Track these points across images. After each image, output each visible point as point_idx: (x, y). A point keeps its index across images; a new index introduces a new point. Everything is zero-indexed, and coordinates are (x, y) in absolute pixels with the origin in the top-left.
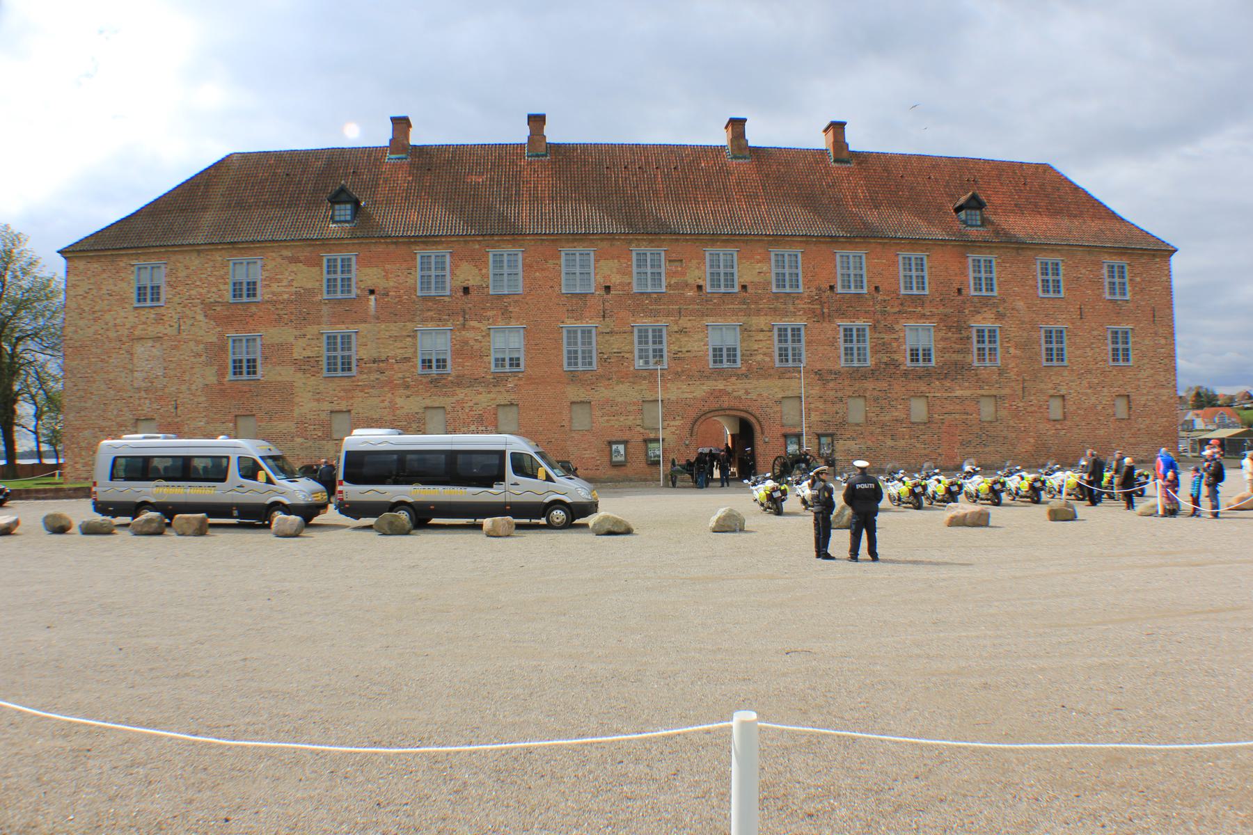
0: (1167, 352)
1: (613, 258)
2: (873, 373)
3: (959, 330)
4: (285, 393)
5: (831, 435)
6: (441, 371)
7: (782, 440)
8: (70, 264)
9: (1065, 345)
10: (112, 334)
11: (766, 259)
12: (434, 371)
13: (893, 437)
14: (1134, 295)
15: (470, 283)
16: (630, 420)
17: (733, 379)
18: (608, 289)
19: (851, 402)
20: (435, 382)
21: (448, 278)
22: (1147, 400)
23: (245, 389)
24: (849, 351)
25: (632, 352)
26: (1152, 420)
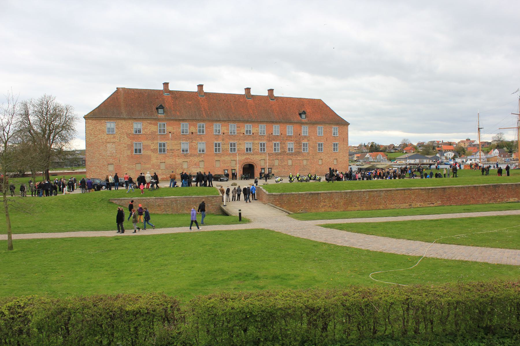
2: (280, 154)
4: (149, 158)
5: (271, 168)
6: (186, 153)
7: (261, 170)
8: (87, 121)
9: (323, 147)
10: (100, 141)
11: (258, 127)
12: (185, 152)
13: (284, 169)
15: (193, 131)
16: (228, 165)
19: (275, 160)
20: (185, 155)
21: (188, 130)
23: (138, 156)
24: (275, 149)
25: (229, 149)
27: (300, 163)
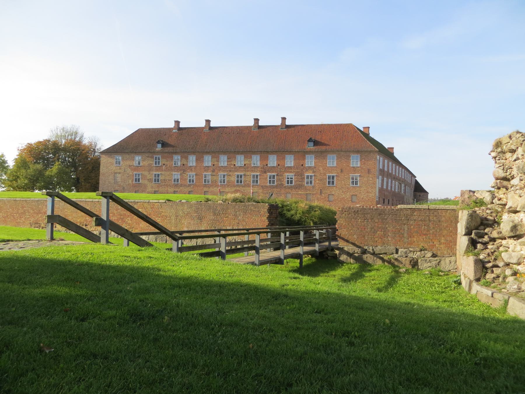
1: (215, 158)
2: (276, 187)
3: (301, 176)
4: (145, 186)
10: (110, 171)
14: (361, 164)
15: (184, 163)
17: (241, 187)
20: (176, 186)
25: (218, 180)
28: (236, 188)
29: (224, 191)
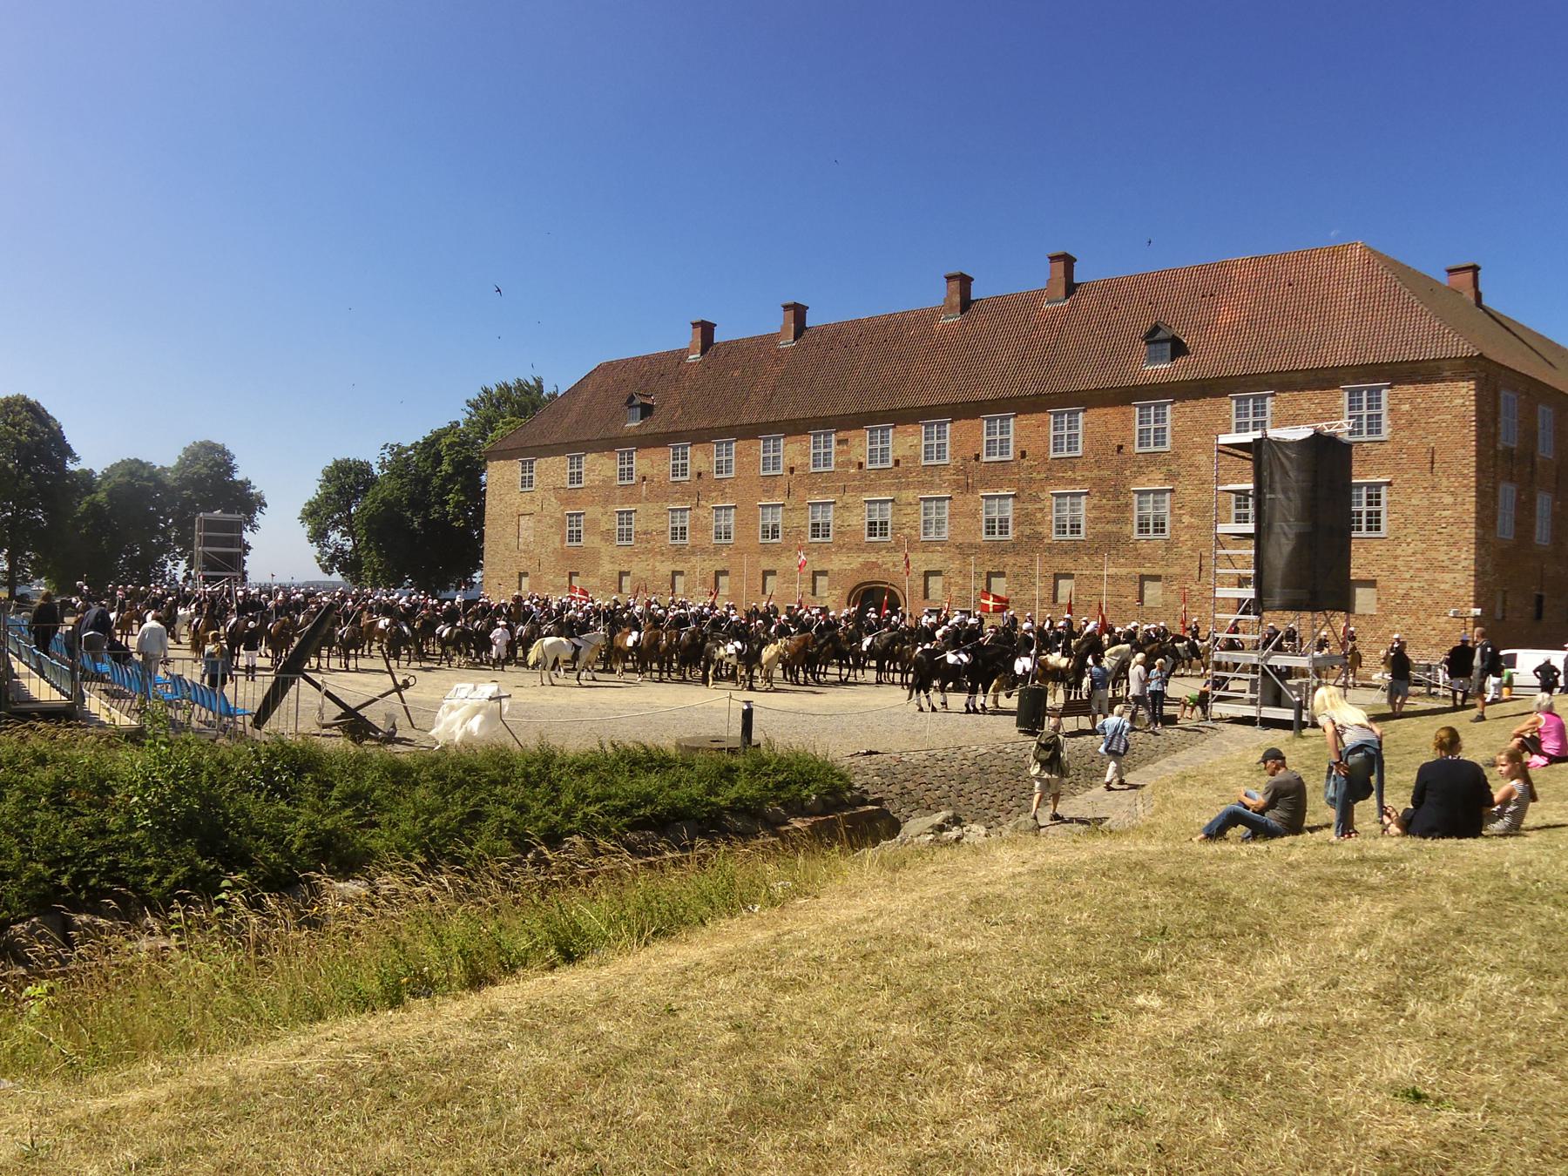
0: (1457, 515)
2: (1015, 548)
4: (595, 555)
10: (509, 511)
14: (1397, 428)
15: (702, 469)
17: (884, 552)
18: (792, 470)
22: (1412, 588)
26: (1418, 618)
27: (1121, 596)
28: (866, 555)
29: (825, 567)
